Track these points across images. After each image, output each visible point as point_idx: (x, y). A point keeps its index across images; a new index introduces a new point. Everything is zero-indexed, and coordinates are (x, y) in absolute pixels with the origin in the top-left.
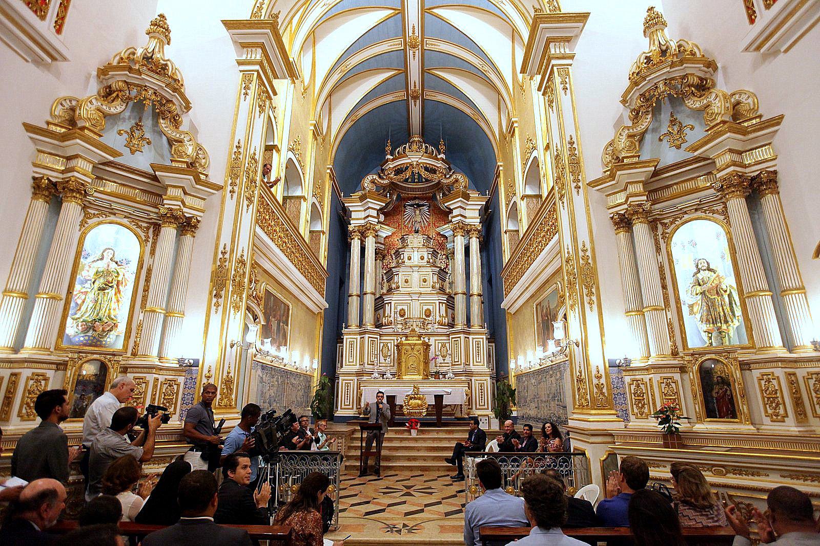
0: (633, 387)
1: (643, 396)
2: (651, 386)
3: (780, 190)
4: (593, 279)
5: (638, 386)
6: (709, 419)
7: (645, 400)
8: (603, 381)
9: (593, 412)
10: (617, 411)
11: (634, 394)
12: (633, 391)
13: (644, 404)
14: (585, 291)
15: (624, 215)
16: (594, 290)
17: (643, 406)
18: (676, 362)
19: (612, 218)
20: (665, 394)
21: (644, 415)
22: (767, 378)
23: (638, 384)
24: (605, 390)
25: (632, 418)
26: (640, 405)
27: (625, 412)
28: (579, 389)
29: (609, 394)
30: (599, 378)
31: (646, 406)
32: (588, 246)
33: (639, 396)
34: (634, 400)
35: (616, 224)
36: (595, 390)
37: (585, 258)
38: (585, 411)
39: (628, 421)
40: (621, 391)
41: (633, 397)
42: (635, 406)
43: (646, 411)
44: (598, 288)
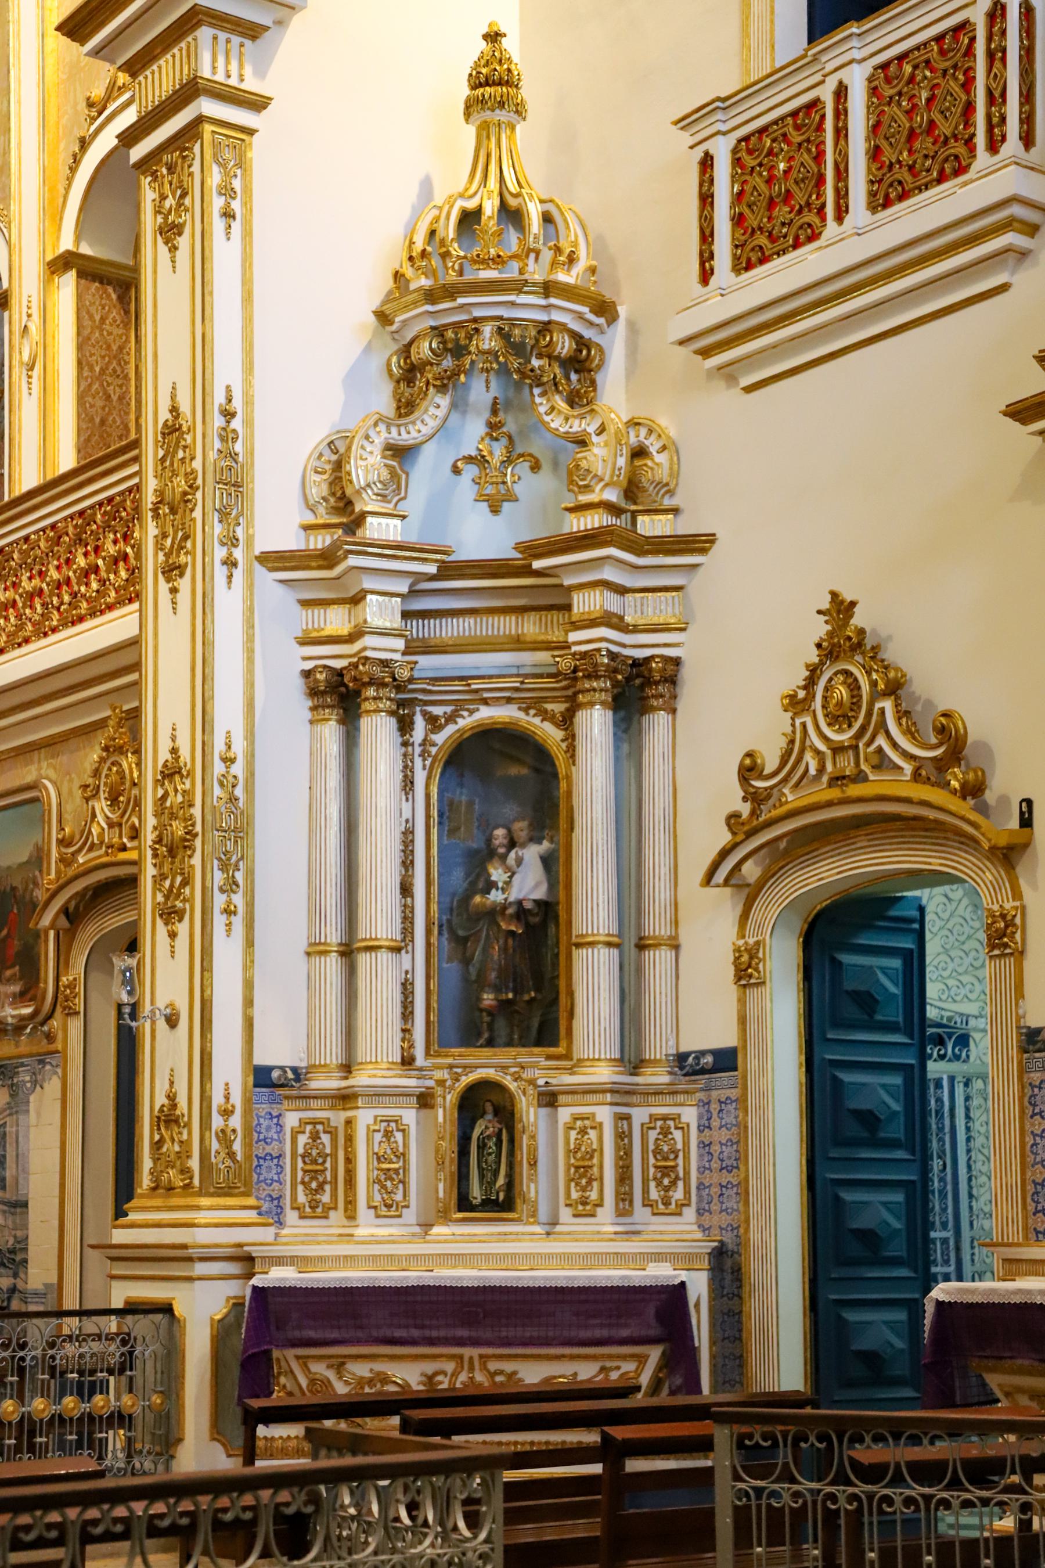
0: (303, 1140)
1: (324, 1162)
2: (350, 1139)
3: (681, 705)
4: (242, 847)
5: (315, 1136)
6: (460, 1215)
7: (328, 1174)
8: (236, 1121)
9: (205, 1201)
10: (258, 1198)
11: (303, 1157)
12: (301, 1150)
13: (325, 1182)
14: (219, 877)
15: (340, 673)
16: (239, 876)
17: (321, 1187)
18: (413, 1082)
19: (307, 674)
20: (378, 1159)
21: (319, 1210)
22: (584, 1125)
23: (318, 1132)
24: (237, 1147)
25: (291, 1216)
26: (314, 1185)
27: (276, 1202)
28: (157, 1145)
29: (248, 1157)
30: (227, 1113)
31: (327, 1187)
32: (239, 748)
33: (314, 1162)
34: (300, 1174)
35: (313, 692)
36: (215, 1145)
37: (228, 783)
38: (175, 1201)
39: (280, 1223)
40: (273, 1149)
41: (300, 1164)
42: (300, 1188)
43: (326, 1198)
44: (250, 874)
